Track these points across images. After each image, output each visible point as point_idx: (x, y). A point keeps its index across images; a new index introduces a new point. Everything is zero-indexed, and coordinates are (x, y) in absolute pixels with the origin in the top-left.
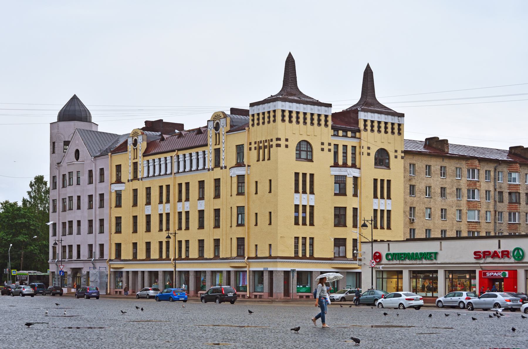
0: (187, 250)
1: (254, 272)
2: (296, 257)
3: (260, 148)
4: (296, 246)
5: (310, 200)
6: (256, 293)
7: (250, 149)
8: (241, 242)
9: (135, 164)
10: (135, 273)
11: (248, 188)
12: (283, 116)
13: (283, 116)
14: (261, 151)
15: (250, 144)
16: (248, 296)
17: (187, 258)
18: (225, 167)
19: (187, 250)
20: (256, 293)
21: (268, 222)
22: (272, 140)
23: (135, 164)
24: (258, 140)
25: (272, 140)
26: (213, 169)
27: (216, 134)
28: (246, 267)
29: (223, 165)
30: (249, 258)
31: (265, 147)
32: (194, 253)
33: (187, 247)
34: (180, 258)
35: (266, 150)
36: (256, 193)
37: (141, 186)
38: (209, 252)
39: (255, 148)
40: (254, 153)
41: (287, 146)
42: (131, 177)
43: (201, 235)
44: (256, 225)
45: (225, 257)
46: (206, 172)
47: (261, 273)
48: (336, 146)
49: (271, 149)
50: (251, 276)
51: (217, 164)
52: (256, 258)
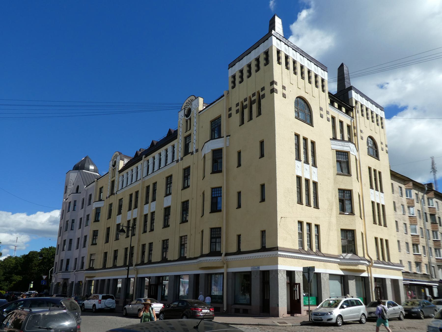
0: (150, 254)
1: (235, 273)
2: (301, 250)
3: (243, 108)
4: (301, 235)
5: (313, 173)
6: (238, 306)
7: (230, 116)
8: (216, 234)
9: (113, 182)
10: (103, 281)
11: (227, 162)
12: (279, 58)
13: (279, 58)
14: (246, 111)
15: (230, 109)
16: (225, 309)
17: (150, 262)
18: (197, 151)
19: (150, 254)
20: (238, 306)
21: (259, 198)
22: (263, 89)
23: (113, 182)
24: (242, 99)
25: (263, 89)
26: (182, 159)
27: (187, 121)
28: (222, 267)
29: (194, 150)
30: (227, 254)
31: (252, 103)
32: (157, 255)
33: (150, 250)
34: (143, 263)
35: (255, 107)
36: (239, 165)
37: (114, 200)
38: (173, 252)
39: (237, 111)
40: (236, 118)
41: (284, 96)
42: (108, 193)
43: (167, 234)
44: (239, 206)
45: (193, 257)
46: (175, 163)
47: (247, 276)
48: (333, 118)
49: (263, 101)
50: (230, 281)
51: (186, 152)
52: (239, 252)
